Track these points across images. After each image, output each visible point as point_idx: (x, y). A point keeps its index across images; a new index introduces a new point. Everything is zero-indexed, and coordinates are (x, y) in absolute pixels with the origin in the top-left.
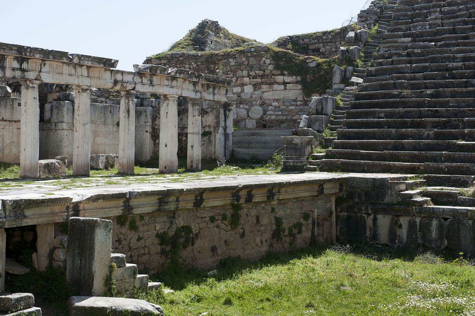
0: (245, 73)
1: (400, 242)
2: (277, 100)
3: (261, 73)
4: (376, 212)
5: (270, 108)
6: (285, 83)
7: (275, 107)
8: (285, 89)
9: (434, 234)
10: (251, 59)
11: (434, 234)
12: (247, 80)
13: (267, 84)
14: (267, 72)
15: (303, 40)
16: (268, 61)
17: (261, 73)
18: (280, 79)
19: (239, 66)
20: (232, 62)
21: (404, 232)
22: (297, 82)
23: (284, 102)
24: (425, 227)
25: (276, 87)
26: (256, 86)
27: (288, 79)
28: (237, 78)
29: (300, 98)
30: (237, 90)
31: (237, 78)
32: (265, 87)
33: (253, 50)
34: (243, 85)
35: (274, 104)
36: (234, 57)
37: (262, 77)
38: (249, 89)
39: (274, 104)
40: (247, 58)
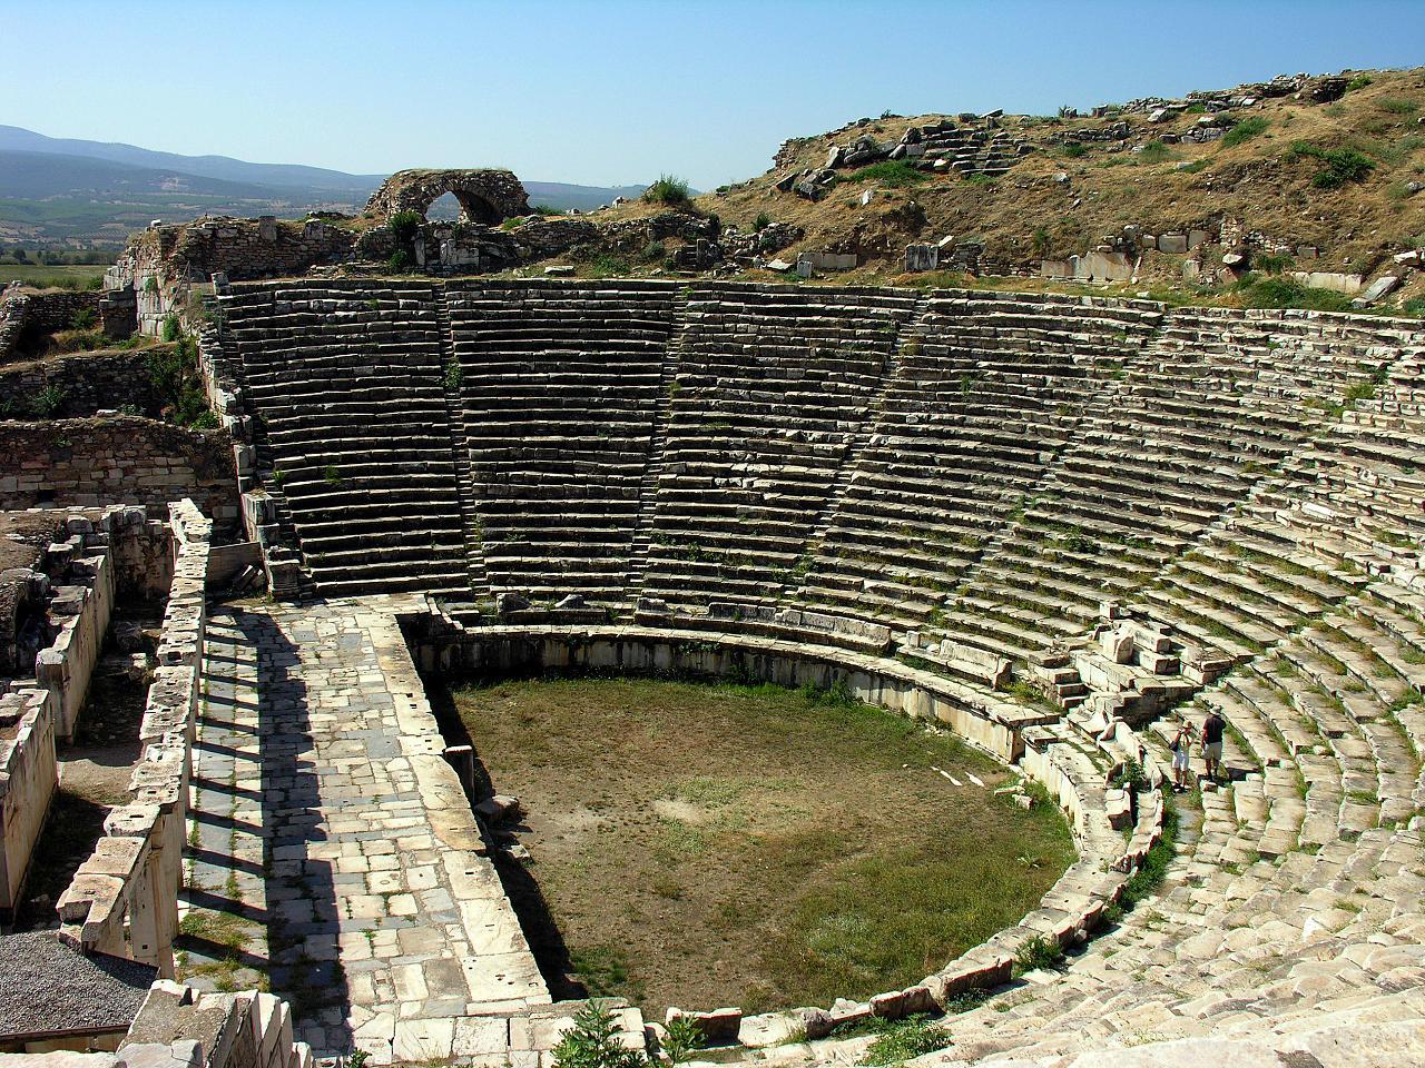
0: (109, 453)
1: (444, 666)
2: (160, 488)
3: (134, 453)
4: (420, 645)
5: (149, 496)
6: (169, 466)
7: (157, 496)
8: (170, 473)
9: (476, 657)
10: (118, 436)
11: (476, 657)
12: (112, 462)
13: (142, 467)
14: (142, 452)
15: (87, 364)
16: (143, 439)
17: (134, 453)
18: (161, 460)
19: (99, 446)
20: (88, 440)
21: (446, 656)
22: (185, 465)
23: (168, 490)
24: (466, 651)
25: (157, 470)
26: (127, 471)
27: (172, 461)
28: (97, 460)
29: (192, 484)
30: (100, 474)
31: (97, 460)
32: (140, 472)
33: (118, 424)
34: (106, 469)
35: (154, 492)
36: (90, 432)
37: (135, 458)
38: (116, 474)
39: (154, 492)
40: (110, 433)
